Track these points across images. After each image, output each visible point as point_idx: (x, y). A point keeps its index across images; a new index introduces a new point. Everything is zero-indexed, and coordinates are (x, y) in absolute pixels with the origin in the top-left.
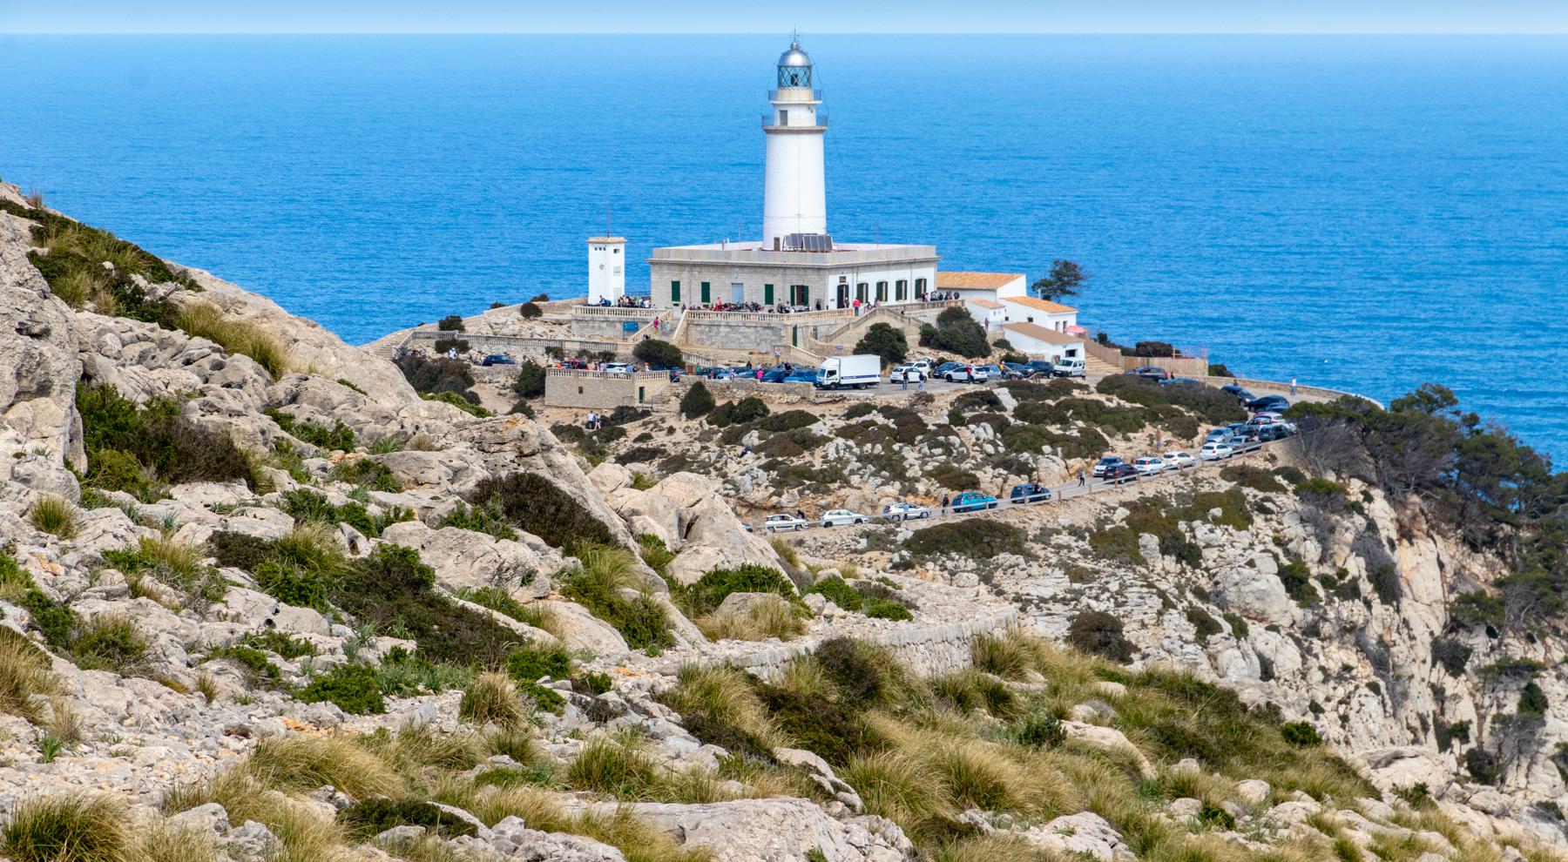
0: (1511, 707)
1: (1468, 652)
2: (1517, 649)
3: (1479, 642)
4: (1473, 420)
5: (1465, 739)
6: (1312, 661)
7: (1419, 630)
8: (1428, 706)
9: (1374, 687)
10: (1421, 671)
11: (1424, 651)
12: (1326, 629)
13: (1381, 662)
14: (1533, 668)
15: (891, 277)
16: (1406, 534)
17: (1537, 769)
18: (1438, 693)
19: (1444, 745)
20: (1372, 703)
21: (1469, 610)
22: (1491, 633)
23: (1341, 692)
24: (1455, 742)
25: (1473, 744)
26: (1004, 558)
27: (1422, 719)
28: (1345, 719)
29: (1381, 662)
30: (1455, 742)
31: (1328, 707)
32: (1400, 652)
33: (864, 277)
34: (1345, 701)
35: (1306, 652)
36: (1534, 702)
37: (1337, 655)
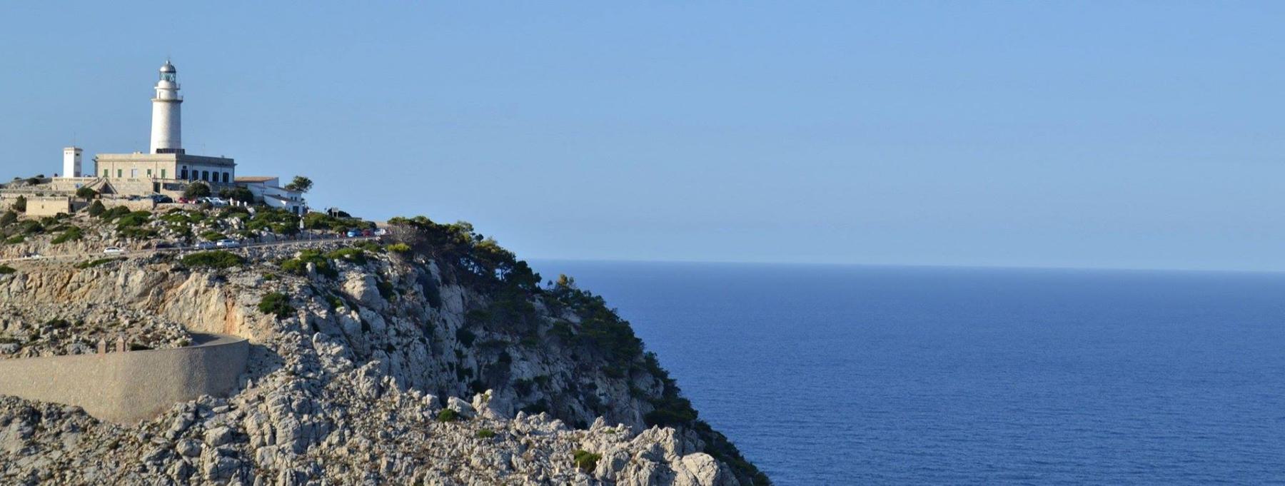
0: (494, 361)
1: (473, 337)
2: (498, 337)
3: (480, 332)
4: (480, 237)
5: (471, 376)
6: (391, 327)
7: (450, 324)
8: (454, 360)
9: (423, 341)
10: (450, 345)
11: (453, 334)
12: (399, 312)
13: (428, 330)
14: (505, 344)
15: (211, 170)
16: (446, 282)
17: (506, 391)
18: (459, 354)
19: (461, 378)
20: (421, 348)
21: (473, 315)
22: (485, 329)
23: (405, 341)
24: (467, 378)
25: (475, 378)
26: (233, 269)
27: (451, 365)
28: (406, 354)
29: (428, 330)
30: (467, 378)
31: (398, 348)
32: (440, 329)
33: (196, 168)
34: (408, 345)
35: (388, 322)
36: (506, 360)
37: (405, 325)
